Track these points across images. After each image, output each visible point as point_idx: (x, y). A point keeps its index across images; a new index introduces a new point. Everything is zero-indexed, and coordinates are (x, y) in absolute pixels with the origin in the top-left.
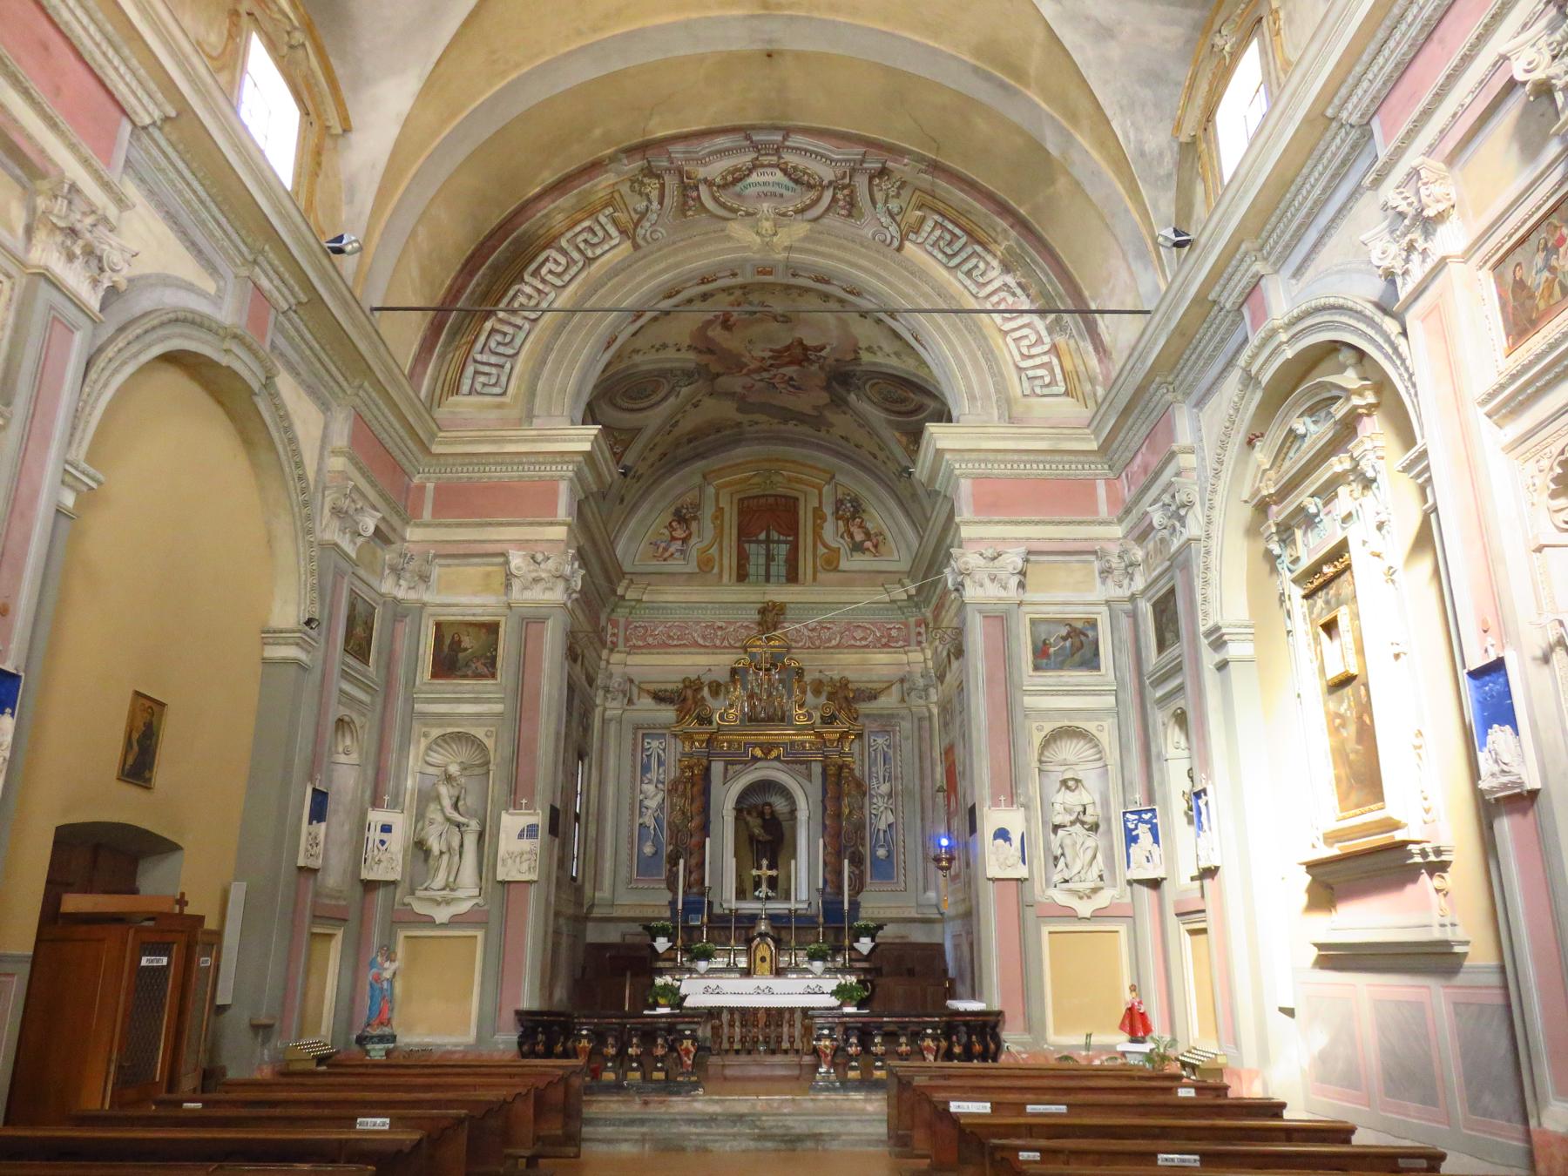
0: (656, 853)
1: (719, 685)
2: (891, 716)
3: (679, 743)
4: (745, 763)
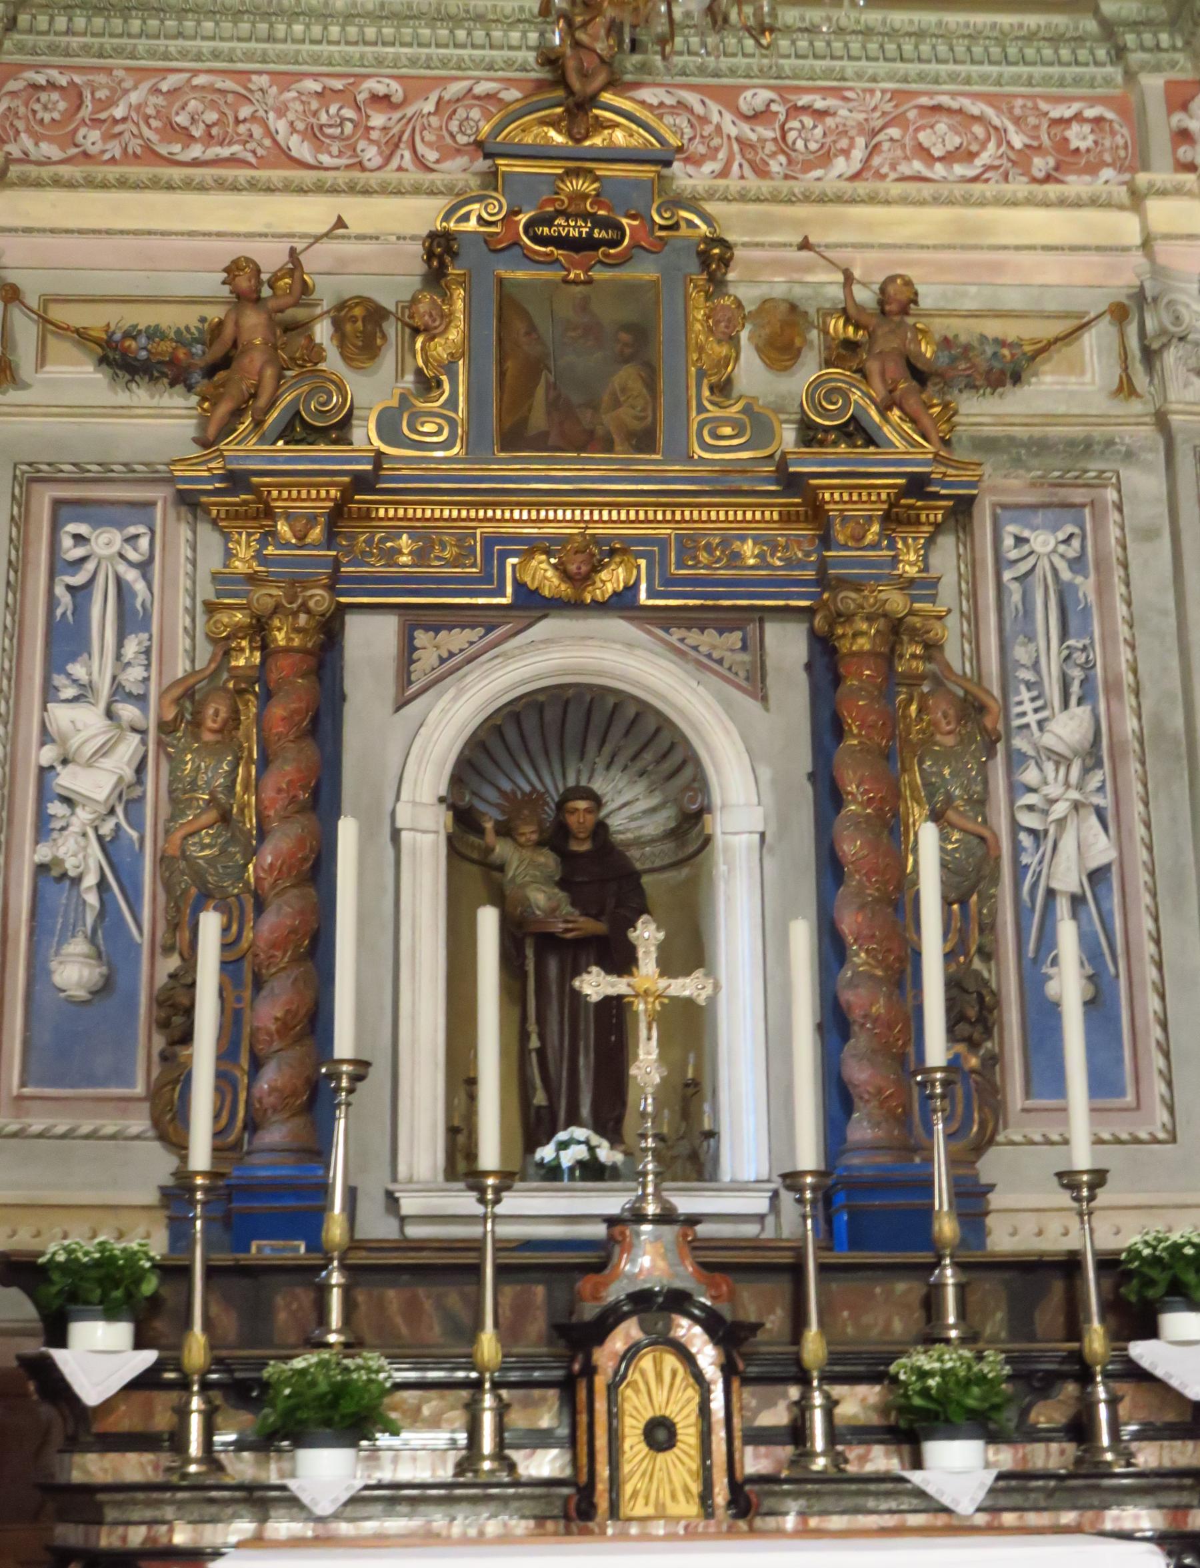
0: (104, 989)
1: (376, 314)
2: (1085, 448)
3: (209, 537)
4: (487, 618)
